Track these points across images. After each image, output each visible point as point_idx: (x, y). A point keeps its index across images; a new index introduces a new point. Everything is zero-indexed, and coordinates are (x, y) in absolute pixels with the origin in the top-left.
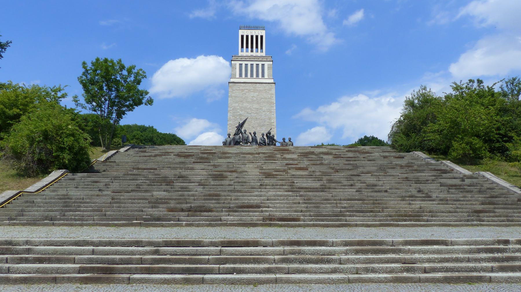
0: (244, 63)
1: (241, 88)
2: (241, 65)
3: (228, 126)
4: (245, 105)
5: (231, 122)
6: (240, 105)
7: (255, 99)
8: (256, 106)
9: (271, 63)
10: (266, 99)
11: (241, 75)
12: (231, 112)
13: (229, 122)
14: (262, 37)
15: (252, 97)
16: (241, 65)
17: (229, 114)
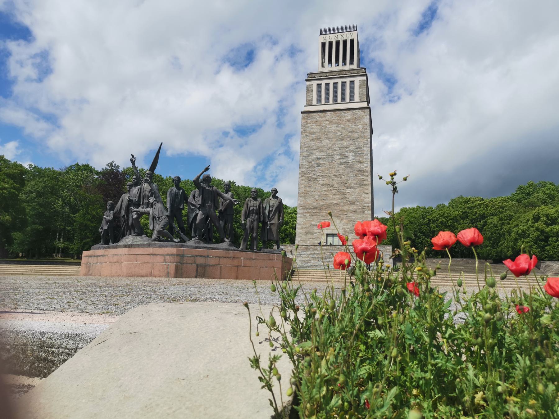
0: (323, 82)
1: (319, 119)
2: (319, 85)
4: (325, 143)
6: (317, 144)
7: (339, 133)
8: (339, 144)
9: (365, 78)
14: (352, 41)
15: (335, 131)
16: (319, 85)
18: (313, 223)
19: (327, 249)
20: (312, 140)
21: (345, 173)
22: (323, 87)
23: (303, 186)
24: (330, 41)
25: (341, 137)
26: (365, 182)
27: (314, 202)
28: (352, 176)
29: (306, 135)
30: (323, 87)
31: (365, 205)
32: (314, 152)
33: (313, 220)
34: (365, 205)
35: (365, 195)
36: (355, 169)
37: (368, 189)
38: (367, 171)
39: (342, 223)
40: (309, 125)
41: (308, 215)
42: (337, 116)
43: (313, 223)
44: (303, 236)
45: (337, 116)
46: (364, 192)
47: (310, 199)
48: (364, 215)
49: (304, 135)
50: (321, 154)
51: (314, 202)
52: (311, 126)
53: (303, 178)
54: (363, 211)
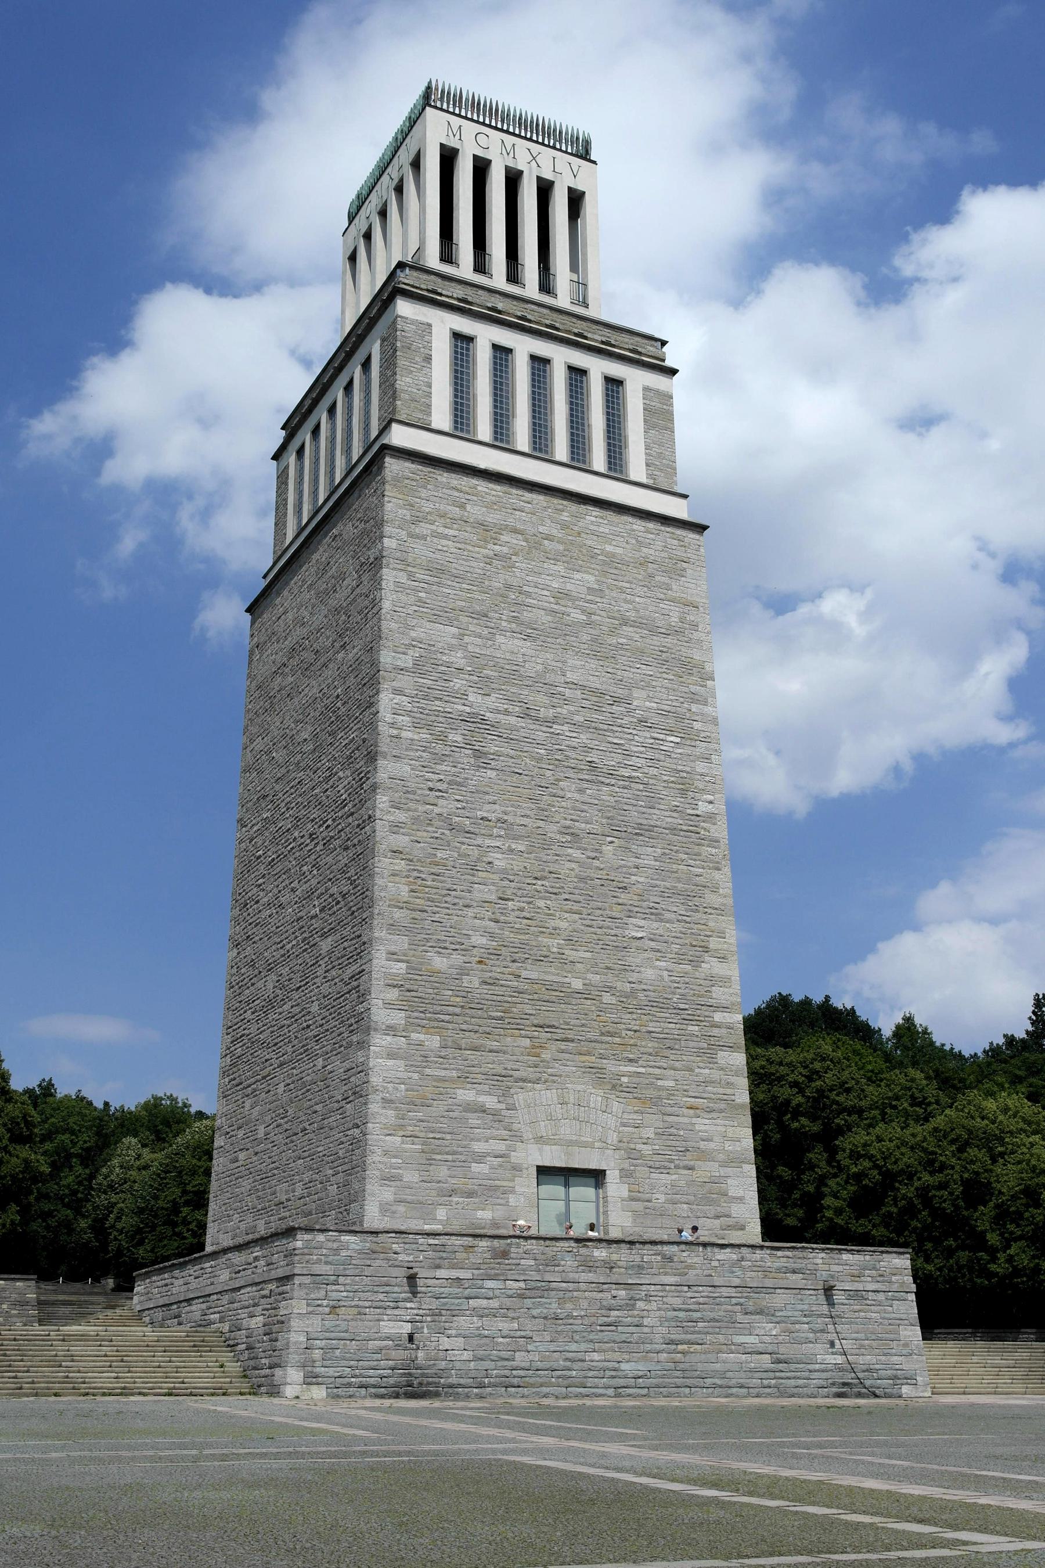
1: (475, 511)
3: (382, 800)
4: (509, 645)
5: (404, 769)
7: (577, 616)
8: (580, 670)
10: (654, 631)
12: (405, 682)
13: (386, 770)
15: (561, 595)
17: (386, 701)
18: (466, 1095)
20: (441, 616)
21: (615, 830)
22: (483, 357)
23: (400, 865)
24: (480, 153)
25: (585, 638)
26: (712, 899)
27: (463, 971)
28: (649, 855)
29: (411, 576)
30: (483, 357)
31: (718, 1017)
32: (458, 683)
33: (464, 1079)
34: (718, 1017)
35: (711, 966)
36: (660, 817)
37: (721, 934)
38: (714, 842)
40: (424, 528)
41: (434, 1042)
42: (564, 526)
43: (466, 1095)
44: (411, 1176)
45: (564, 526)
46: (706, 950)
47: (441, 948)
48: (716, 1075)
49: (403, 578)
50: (492, 701)
51: (463, 971)
52: (436, 535)
53: (401, 816)
54: (710, 1051)
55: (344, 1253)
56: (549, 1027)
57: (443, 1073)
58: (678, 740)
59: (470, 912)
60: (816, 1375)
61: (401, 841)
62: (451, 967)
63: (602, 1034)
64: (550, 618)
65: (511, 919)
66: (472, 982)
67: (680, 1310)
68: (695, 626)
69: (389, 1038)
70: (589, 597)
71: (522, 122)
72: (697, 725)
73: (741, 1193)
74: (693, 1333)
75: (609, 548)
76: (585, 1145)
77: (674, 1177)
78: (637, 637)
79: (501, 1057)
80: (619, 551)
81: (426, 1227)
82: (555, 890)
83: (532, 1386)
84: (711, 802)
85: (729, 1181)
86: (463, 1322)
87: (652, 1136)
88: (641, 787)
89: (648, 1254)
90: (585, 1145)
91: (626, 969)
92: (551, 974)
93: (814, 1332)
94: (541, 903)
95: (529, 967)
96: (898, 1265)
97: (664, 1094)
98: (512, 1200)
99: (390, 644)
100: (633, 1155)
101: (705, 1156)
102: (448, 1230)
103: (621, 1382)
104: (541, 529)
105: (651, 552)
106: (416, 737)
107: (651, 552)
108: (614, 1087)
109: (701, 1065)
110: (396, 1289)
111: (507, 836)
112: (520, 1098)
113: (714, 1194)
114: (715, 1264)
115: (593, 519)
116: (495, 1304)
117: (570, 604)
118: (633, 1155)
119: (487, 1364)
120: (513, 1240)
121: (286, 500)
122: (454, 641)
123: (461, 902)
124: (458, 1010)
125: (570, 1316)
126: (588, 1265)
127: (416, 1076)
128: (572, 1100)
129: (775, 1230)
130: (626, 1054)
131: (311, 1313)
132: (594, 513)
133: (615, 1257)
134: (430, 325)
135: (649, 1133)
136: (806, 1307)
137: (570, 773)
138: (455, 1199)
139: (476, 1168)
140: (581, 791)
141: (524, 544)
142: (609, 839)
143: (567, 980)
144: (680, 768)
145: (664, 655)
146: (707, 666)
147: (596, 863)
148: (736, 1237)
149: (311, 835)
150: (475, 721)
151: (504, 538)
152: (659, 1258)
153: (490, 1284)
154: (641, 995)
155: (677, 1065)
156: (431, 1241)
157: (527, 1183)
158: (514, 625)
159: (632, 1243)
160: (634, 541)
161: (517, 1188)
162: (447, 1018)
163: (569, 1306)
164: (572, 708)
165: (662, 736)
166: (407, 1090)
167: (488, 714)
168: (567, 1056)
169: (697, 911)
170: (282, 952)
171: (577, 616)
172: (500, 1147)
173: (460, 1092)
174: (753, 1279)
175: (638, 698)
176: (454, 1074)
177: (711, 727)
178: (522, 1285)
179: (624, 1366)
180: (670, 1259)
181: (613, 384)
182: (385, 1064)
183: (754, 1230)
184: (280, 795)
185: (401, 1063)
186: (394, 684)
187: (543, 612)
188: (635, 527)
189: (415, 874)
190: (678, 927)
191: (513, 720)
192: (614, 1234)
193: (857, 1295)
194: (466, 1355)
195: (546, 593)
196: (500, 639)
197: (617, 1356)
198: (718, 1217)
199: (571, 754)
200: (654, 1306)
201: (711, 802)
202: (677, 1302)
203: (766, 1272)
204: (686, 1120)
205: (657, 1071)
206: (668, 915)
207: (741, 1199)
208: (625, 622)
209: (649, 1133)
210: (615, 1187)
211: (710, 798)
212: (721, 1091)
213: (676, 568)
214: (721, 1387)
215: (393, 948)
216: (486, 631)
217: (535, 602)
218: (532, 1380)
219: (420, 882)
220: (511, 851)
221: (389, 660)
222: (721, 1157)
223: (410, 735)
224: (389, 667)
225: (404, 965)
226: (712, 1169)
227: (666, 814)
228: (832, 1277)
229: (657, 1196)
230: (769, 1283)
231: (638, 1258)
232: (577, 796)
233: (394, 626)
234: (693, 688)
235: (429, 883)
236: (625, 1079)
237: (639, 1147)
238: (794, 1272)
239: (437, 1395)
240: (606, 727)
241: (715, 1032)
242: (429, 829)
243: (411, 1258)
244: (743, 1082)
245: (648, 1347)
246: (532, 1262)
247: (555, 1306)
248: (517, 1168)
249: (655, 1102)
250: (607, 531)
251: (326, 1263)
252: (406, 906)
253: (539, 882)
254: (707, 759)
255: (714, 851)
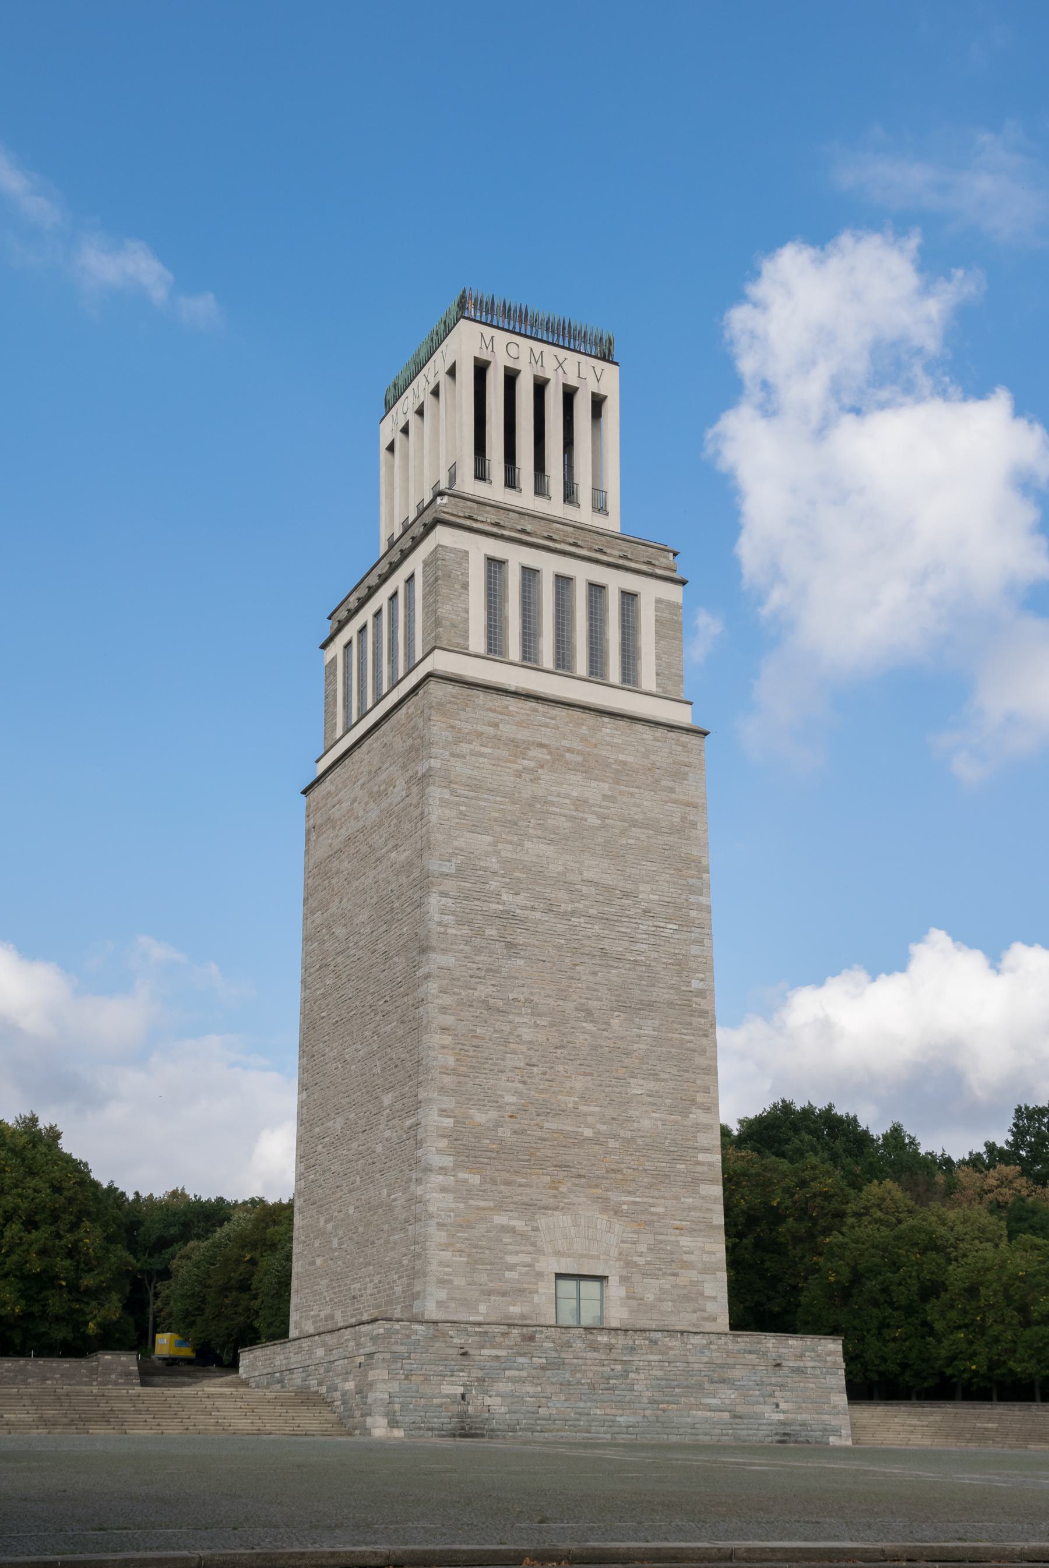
4: (535, 849)
5: (449, 960)
7: (593, 820)
11: (495, 647)
12: (449, 885)
13: (437, 960)
15: (581, 803)
17: (434, 902)
18: (501, 1219)
19: (610, 1348)
23: (447, 1040)
27: (498, 1125)
31: (701, 1157)
32: (494, 884)
33: (499, 1208)
34: (701, 1157)
39: (617, 1228)
41: (476, 1179)
43: (501, 1219)
45: (584, 739)
46: (693, 1102)
48: (698, 1202)
50: (521, 900)
51: (498, 1125)
53: (447, 1000)
54: (693, 1183)
55: (413, 1337)
56: (565, 1166)
57: (482, 1204)
58: (676, 927)
59: (503, 1077)
60: (764, 1427)
61: (449, 1020)
62: (489, 1120)
63: (608, 1172)
64: (569, 824)
65: (536, 1080)
66: (504, 1132)
67: (662, 1379)
68: (694, 825)
69: (441, 1177)
70: (604, 803)
71: (549, 326)
72: (693, 914)
73: (714, 1294)
74: (672, 1396)
75: (622, 757)
76: (593, 1257)
77: (662, 1281)
78: (643, 837)
79: (528, 1191)
80: (630, 759)
81: (472, 1319)
82: (572, 1057)
83: (551, 1431)
84: (702, 980)
85: (706, 1285)
86: (502, 1387)
87: (645, 1250)
88: (644, 968)
89: (639, 1340)
90: (593, 1257)
91: (629, 1120)
92: (568, 1126)
93: (762, 1396)
94: (560, 1068)
95: (550, 1119)
96: (832, 1348)
97: (655, 1218)
98: (536, 1298)
99: (437, 853)
100: (629, 1264)
101: (686, 1265)
102: (488, 1320)
103: (616, 1429)
104: (564, 743)
105: (659, 758)
106: (459, 933)
107: (659, 758)
108: (616, 1213)
109: (687, 1194)
110: (453, 1363)
111: (533, 1014)
112: (542, 1221)
113: (692, 1296)
114: (689, 1346)
115: (608, 731)
116: (524, 1374)
117: (587, 810)
118: (629, 1264)
119: (517, 1416)
120: (539, 1329)
121: (335, 691)
122: (490, 849)
123: (496, 1068)
124: (494, 1155)
125: (579, 1383)
126: (594, 1347)
127: (462, 1206)
128: (583, 1224)
129: (738, 1324)
130: (626, 1188)
131: (392, 1378)
132: (609, 726)
133: (613, 1341)
134: (467, 553)
135: (643, 1248)
136: (758, 1379)
137: (586, 959)
138: (493, 1298)
139: (508, 1275)
140: (595, 973)
141: (549, 757)
142: (616, 1014)
143: (580, 1130)
144: (677, 951)
145: (666, 852)
146: (703, 860)
147: (605, 1033)
148: (709, 1327)
149: (371, 1006)
150: (507, 917)
151: (532, 753)
152: (647, 1342)
153: (521, 1360)
154: (639, 1141)
155: (667, 1195)
156: (477, 1329)
157: (547, 1287)
158: (539, 832)
159: (626, 1331)
160: (643, 750)
161: (540, 1290)
162: (486, 1160)
163: (579, 1375)
164: (587, 903)
165: (662, 924)
166: (455, 1216)
167: (518, 911)
168: (580, 1189)
169: (688, 1072)
170: (347, 1099)
171: (593, 820)
172: (528, 1259)
173: (496, 1218)
174: (718, 1357)
175: (643, 892)
176: (491, 1204)
177: (704, 915)
178: (544, 1361)
179: (618, 1419)
180: (656, 1343)
181: (629, 597)
182: (437, 1196)
183: (723, 1321)
184: (341, 967)
185: (450, 1197)
186: (441, 888)
187: (564, 819)
188: (645, 736)
189: (460, 1046)
190: (672, 1084)
191: (538, 915)
192: (615, 1324)
193: (799, 1371)
194: (503, 1410)
195: (568, 801)
196: (528, 844)
197: (614, 1411)
198: (694, 1312)
199: (587, 942)
200: (642, 1376)
201: (702, 980)
202: (660, 1373)
203: (728, 1353)
204: (672, 1238)
205: (651, 1200)
206: (663, 1076)
207: (714, 1298)
208: (634, 824)
209: (643, 1248)
210: (615, 1290)
211: (702, 976)
212: (702, 1215)
213: (679, 773)
214: (691, 1434)
215: (443, 1106)
216: (516, 839)
217: (557, 810)
218: (552, 1427)
219: (463, 1052)
220: (536, 1025)
221: (436, 868)
222: (700, 1266)
223: (454, 932)
224: (436, 874)
225: (451, 1120)
226: (693, 1275)
227: (665, 991)
228: (780, 1357)
229: (649, 1296)
230: (730, 1361)
231: (631, 1343)
232: (591, 978)
233: (440, 837)
234: (691, 881)
235: (471, 1054)
236: (625, 1207)
237: (635, 1259)
238: (750, 1352)
239: (482, 1436)
240: (615, 918)
241: (699, 1168)
242: (471, 1009)
243: (463, 1341)
244: (720, 1208)
245: (637, 1406)
246: (552, 1345)
247: (567, 1375)
248: (540, 1275)
249: (649, 1223)
250: (620, 741)
251: (401, 1344)
252: (454, 1072)
253: (559, 1051)
254: (700, 942)
255: (702, 1021)
